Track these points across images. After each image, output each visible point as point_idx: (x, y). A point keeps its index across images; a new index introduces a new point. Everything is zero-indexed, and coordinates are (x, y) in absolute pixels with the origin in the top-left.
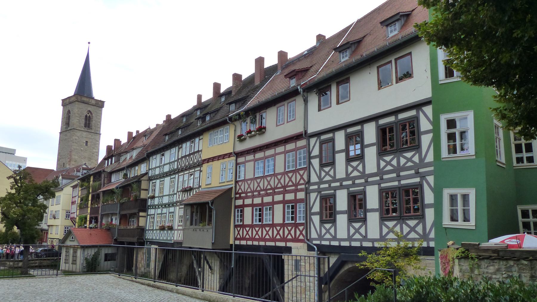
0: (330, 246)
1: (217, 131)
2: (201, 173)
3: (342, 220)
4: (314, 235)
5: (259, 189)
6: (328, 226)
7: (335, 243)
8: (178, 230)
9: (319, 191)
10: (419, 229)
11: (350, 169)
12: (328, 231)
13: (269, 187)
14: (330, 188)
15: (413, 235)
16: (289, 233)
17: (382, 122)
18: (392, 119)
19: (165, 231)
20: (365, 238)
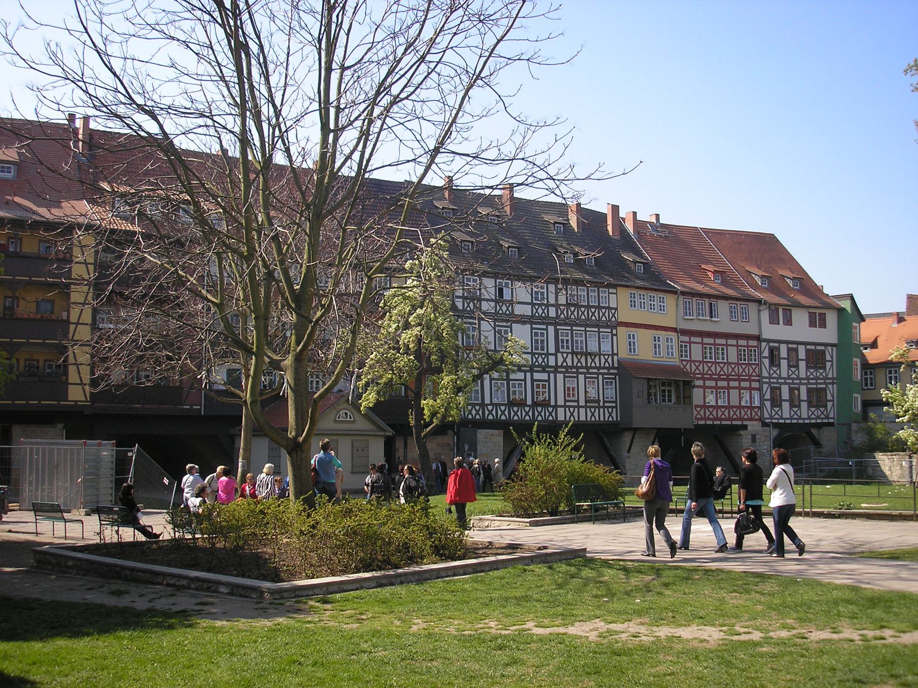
0: (778, 423)
1: (644, 295)
2: (615, 338)
3: (786, 406)
4: (766, 415)
5: (710, 372)
6: (776, 409)
7: (782, 421)
8: (565, 406)
9: (770, 383)
10: (825, 413)
11: (790, 373)
12: (777, 413)
13: (722, 373)
14: (777, 383)
15: (822, 416)
16: (746, 413)
17: (808, 347)
18: (813, 347)
19: (527, 409)
20: (800, 418)
